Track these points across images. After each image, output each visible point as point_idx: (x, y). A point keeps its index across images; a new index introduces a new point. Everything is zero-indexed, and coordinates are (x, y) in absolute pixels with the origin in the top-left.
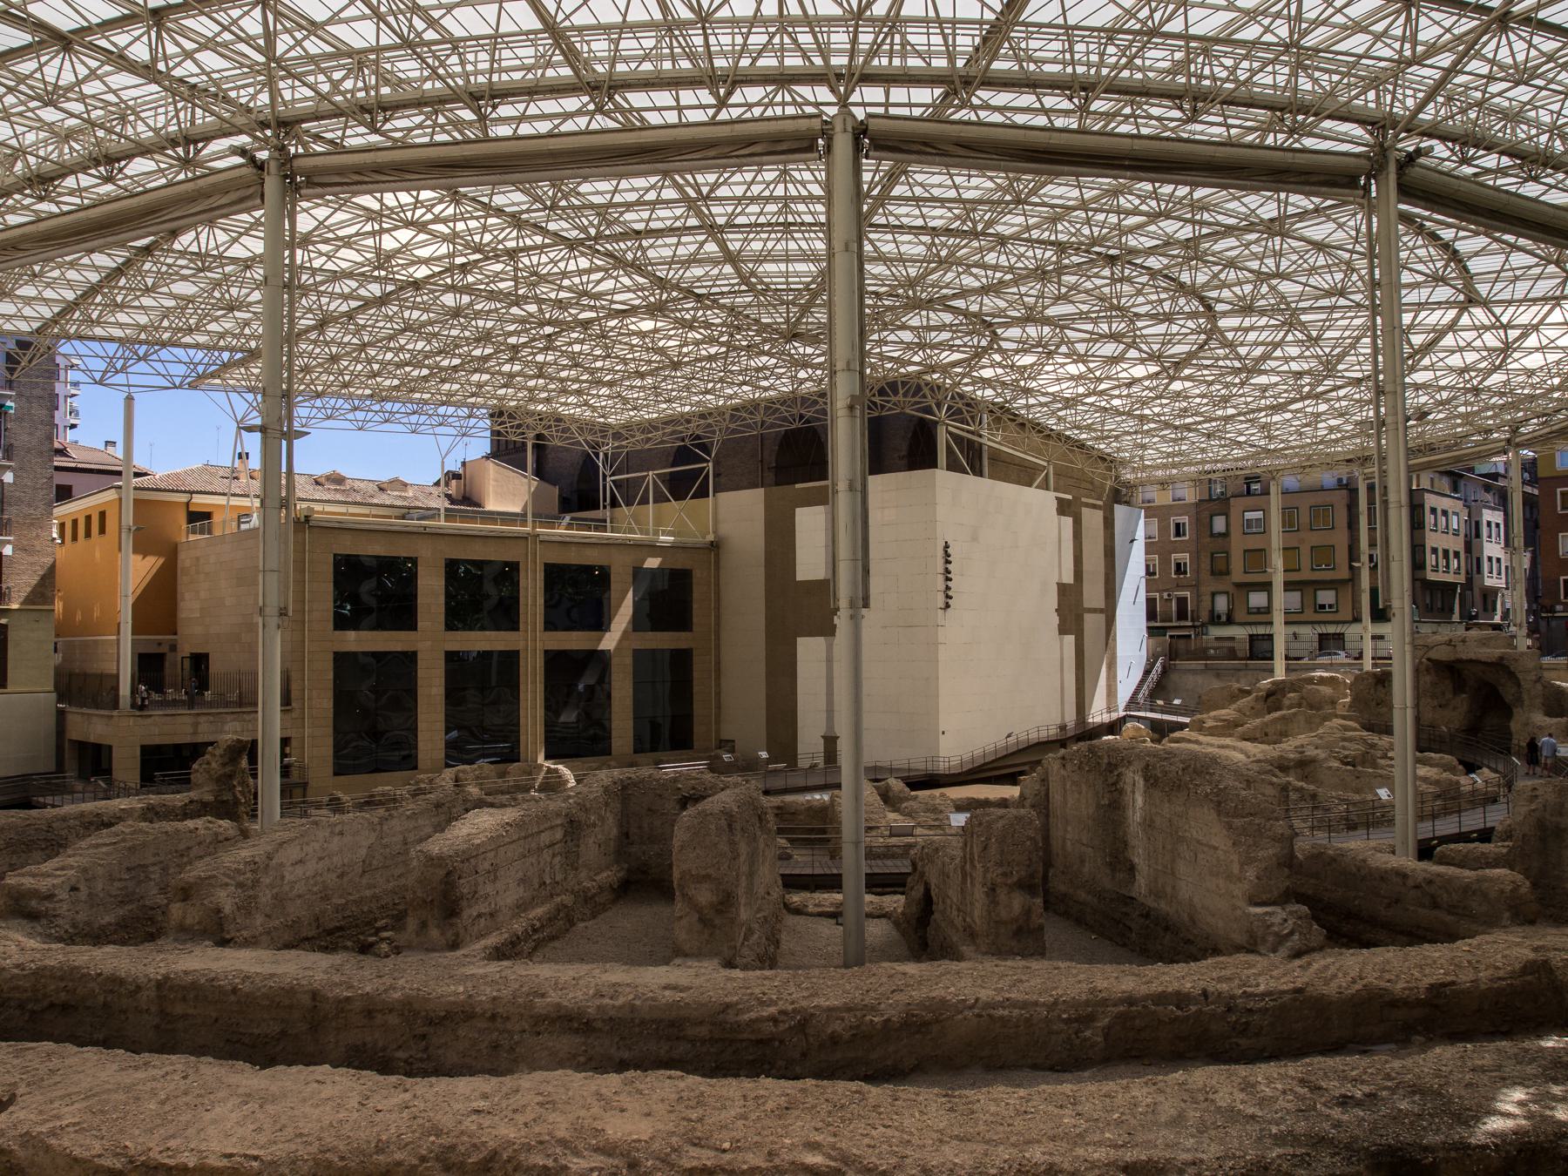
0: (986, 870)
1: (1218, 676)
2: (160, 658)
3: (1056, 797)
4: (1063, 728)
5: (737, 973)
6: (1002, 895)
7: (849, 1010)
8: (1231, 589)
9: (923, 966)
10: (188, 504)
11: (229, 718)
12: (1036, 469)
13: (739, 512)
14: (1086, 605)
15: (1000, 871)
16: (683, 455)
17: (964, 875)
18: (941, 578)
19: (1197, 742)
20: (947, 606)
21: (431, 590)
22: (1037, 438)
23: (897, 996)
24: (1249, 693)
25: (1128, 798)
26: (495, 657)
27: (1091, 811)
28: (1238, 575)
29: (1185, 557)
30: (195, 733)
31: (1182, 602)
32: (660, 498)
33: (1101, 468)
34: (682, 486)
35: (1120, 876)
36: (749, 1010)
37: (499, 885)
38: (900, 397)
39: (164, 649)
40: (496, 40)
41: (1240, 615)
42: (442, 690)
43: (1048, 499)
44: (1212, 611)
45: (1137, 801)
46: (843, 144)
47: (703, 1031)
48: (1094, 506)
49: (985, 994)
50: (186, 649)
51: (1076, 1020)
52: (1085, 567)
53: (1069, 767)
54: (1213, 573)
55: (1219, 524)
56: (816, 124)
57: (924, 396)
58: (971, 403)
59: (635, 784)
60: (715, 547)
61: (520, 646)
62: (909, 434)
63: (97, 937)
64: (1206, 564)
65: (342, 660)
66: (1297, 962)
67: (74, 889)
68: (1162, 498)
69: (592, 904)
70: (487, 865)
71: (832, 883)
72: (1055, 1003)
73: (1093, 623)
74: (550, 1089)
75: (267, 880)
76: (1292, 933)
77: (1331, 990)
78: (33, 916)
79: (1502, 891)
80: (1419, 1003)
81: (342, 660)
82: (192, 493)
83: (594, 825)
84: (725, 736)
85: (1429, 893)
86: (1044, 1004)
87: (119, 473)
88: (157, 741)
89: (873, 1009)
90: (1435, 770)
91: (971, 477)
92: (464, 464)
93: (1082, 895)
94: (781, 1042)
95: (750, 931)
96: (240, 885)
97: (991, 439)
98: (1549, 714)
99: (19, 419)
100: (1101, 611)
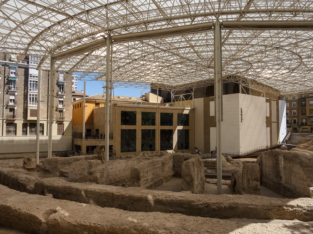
0: (247, 176)
1: (303, 136)
2: (91, 130)
3: (264, 161)
4: (267, 147)
5: (194, 194)
6: (251, 182)
7: (217, 204)
9: (233, 195)
10: (95, 102)
12: (262, 93)
15: (251, 176)
16: (187, 91)
17: (243, 177)
19: (298, 150)
20: (242, 121)
21: (139, 118)
22: (261, 86)
23: (228, 201)
25: (280, 162)
26: (151, 131)
27: (272, 164)
29: (295, 111)
30: (96, 144)
31: (295, 121)
32: (183, 100)
33: (276, 92)
36: (197, 202)
37: (148, 175)
38: (231, 79)
40: (148, 11)
41: (309, 123)
42: (141, 137)
44: (302, 122)
45: (282, 163)
46: (217, 27)
48: (274, 100)
49: (247, 202)
50: (95, 128)
53: (267, 155)
54: (302, 114)
56: (212, 24)
57: (237, 78)
59: (176, 156)
61: (156, 129)
62: (233, 86)
63: (76, 181)
64: (300, 112)
65: (122, 131)
67: (72, 172)
69: (167, 179)
70: (146, 171)
71: (215, 177)
72: (263, 205)
73: (274, 125)
74: (156, 215)
75: (105, 172)
78: (65, 177)
81: (122, 131)
83: (167, 164)
84: (196, 147)
86: (260, 205)
87: (83, 96)
88: (89, 145)
89: (222, 204)
92: (145, 94)
93: (270, 182)
95: (197, 186)
96: (101, 172)
97: (251, 87)
99: (66, 86)
100: (276, 122)
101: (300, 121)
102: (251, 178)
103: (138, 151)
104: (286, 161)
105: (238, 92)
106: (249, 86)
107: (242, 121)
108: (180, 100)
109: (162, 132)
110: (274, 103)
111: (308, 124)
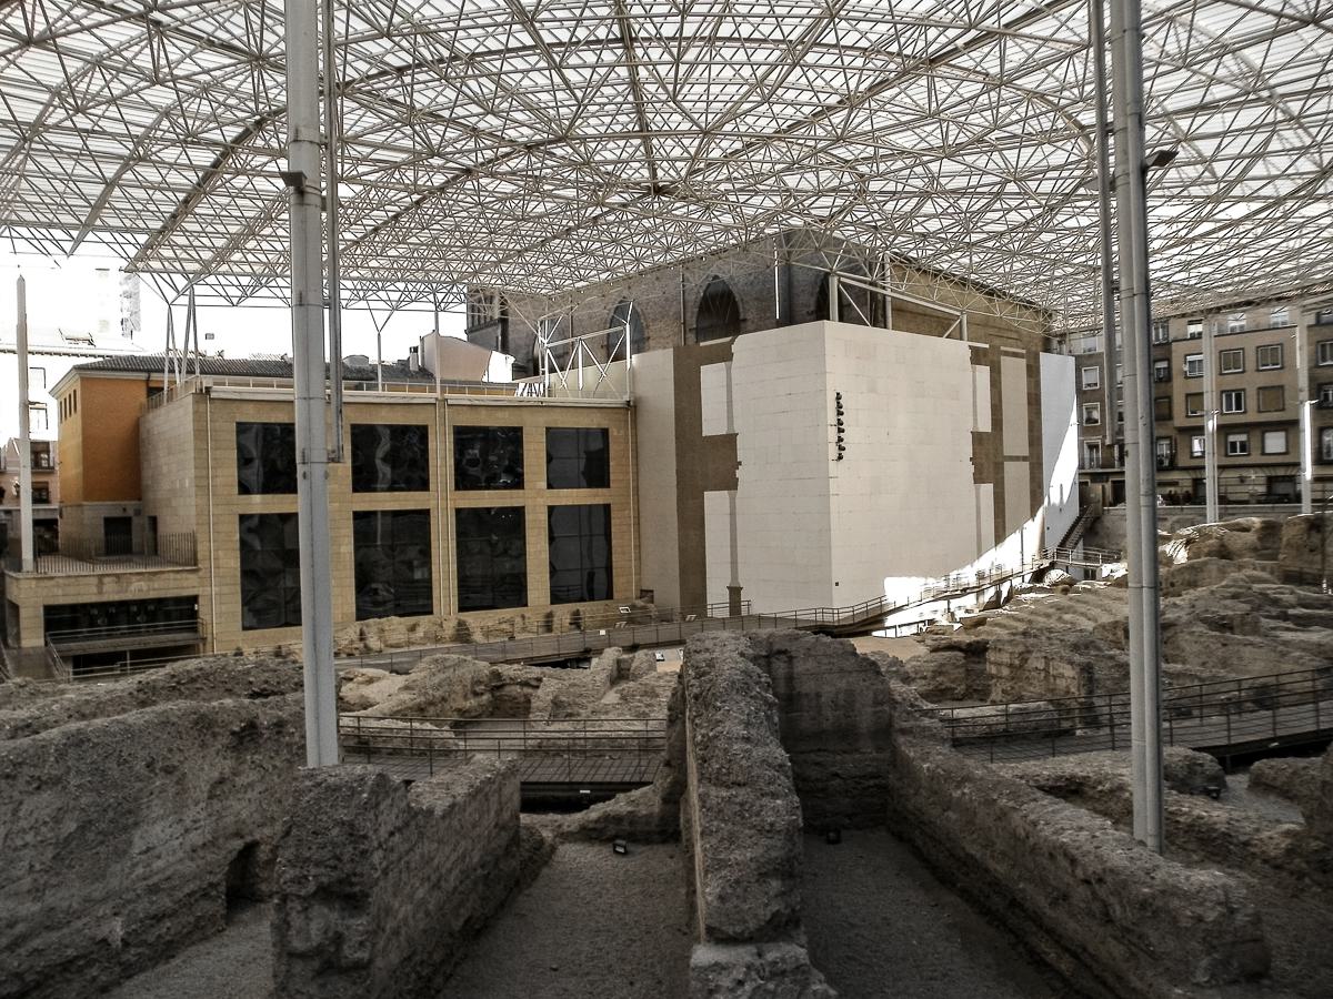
2: (126, 521)
8: (1173, 433)
11: (134, 578)
13: (651, 370)
14: (1007, 452)
18: (835, 429)
20: (840, 457)
26: (379, 516)
28: (1180, 420)
39: (130, 513)
41: (1183, 461)
43: (960, 349)
48: (1015, 355)
52: (971, 418)
59: (207, 676)
60: (632, 408)
62: (807, 286)
73: (1016, 474)
79: (1200, 919)
82: (149, 371)
91: (870, 329)
97: (893, 289)
102: (294, 889)
106: (884, 288)
107: (840, 457)
109: (468, 521)
110: (1014, 370)
111: (1180, 464)
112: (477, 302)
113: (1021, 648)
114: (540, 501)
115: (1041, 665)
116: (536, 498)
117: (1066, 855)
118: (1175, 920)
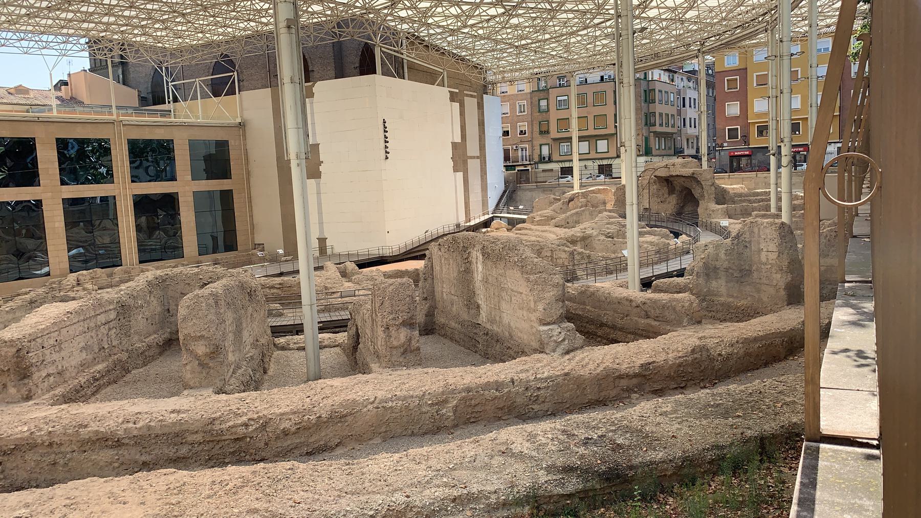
0: (383, 317)
4: (458, 226)
7: (295, 413)
8: (550, 141)
15: (391, 317)
16: (217, 68)
17: (373, 320)
19: (530, 229)
20: (387, 158)
23: (325, 401)
24: (559, 200)
25: (474, 266)
27: (455, 274)
28: (554, 134)
32: (204, 96)
34: (218, 89)
35: (473, 312)
37: (63, 354)
41: (555, 157)
45: (479, 268)
47: (199, 437)
48: (472, 96)
49: (380, 394)
51: (437, 404)
53: (442, 250)
55: (543, 103)
58: (395, 33)
59: (172, 278)
60: (242, 126)
64: (536, 129)
66: (567, 357)
68: (512, 90)
69: (145, 358)
70: (52, 342)
71: (298, 329)
74: (77, 493)
76: (564, 340)
77: (585, 372)
80: (636, 376)
83: (142, 307)
85: (644, 309)
90: (657, 237)
93: (453, 324)
94: (251, 438)
97: (407, 56)
98: (718, 203)
100: (478, 157)
101: (537, 152)
103: (58, 273)
104: (489, 263)
105: (374, 72)
107: (387, 158)
108: (195, 98)
109: (142, 204)
112: (94, 44)
113: (538, 247)
114: (187, 188)
115: (549, 254)
116: (186, 186)
117: (627, 300)
118: (674, 309)
